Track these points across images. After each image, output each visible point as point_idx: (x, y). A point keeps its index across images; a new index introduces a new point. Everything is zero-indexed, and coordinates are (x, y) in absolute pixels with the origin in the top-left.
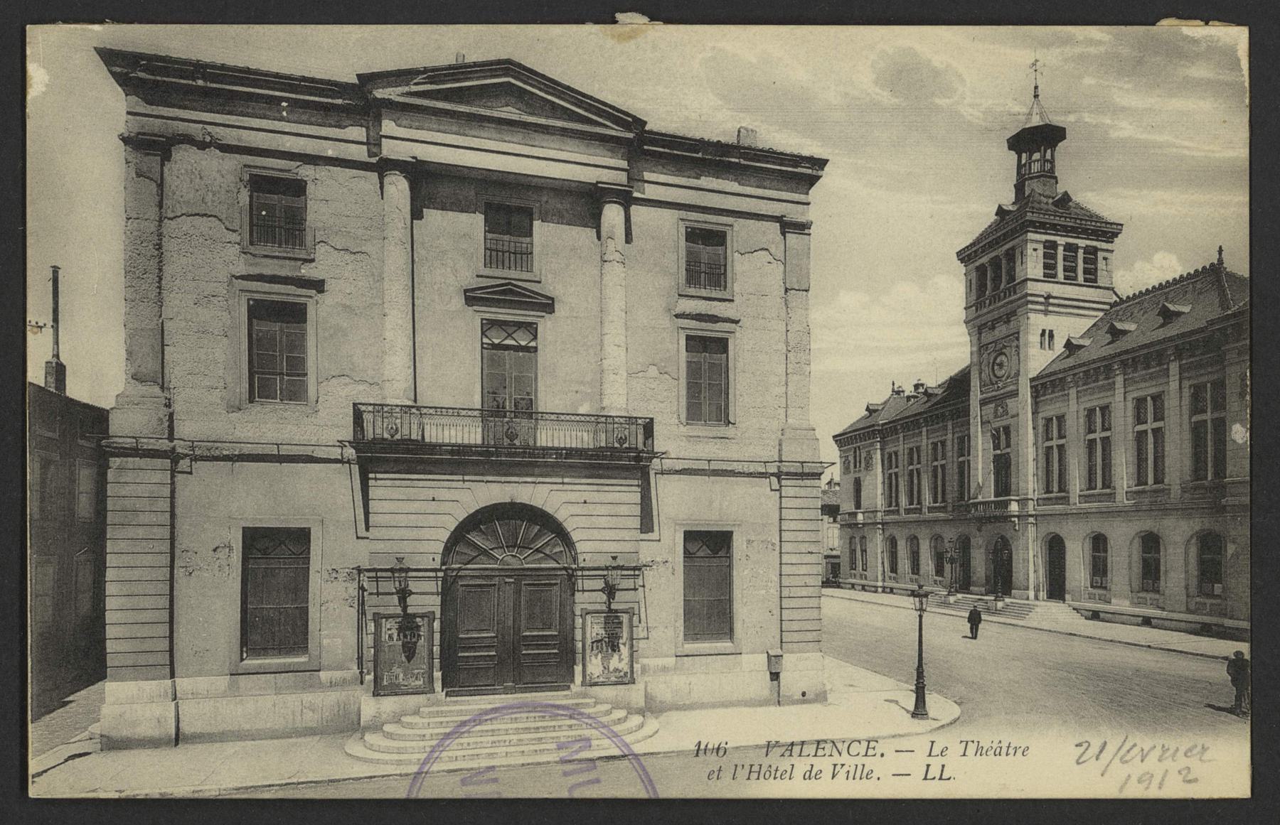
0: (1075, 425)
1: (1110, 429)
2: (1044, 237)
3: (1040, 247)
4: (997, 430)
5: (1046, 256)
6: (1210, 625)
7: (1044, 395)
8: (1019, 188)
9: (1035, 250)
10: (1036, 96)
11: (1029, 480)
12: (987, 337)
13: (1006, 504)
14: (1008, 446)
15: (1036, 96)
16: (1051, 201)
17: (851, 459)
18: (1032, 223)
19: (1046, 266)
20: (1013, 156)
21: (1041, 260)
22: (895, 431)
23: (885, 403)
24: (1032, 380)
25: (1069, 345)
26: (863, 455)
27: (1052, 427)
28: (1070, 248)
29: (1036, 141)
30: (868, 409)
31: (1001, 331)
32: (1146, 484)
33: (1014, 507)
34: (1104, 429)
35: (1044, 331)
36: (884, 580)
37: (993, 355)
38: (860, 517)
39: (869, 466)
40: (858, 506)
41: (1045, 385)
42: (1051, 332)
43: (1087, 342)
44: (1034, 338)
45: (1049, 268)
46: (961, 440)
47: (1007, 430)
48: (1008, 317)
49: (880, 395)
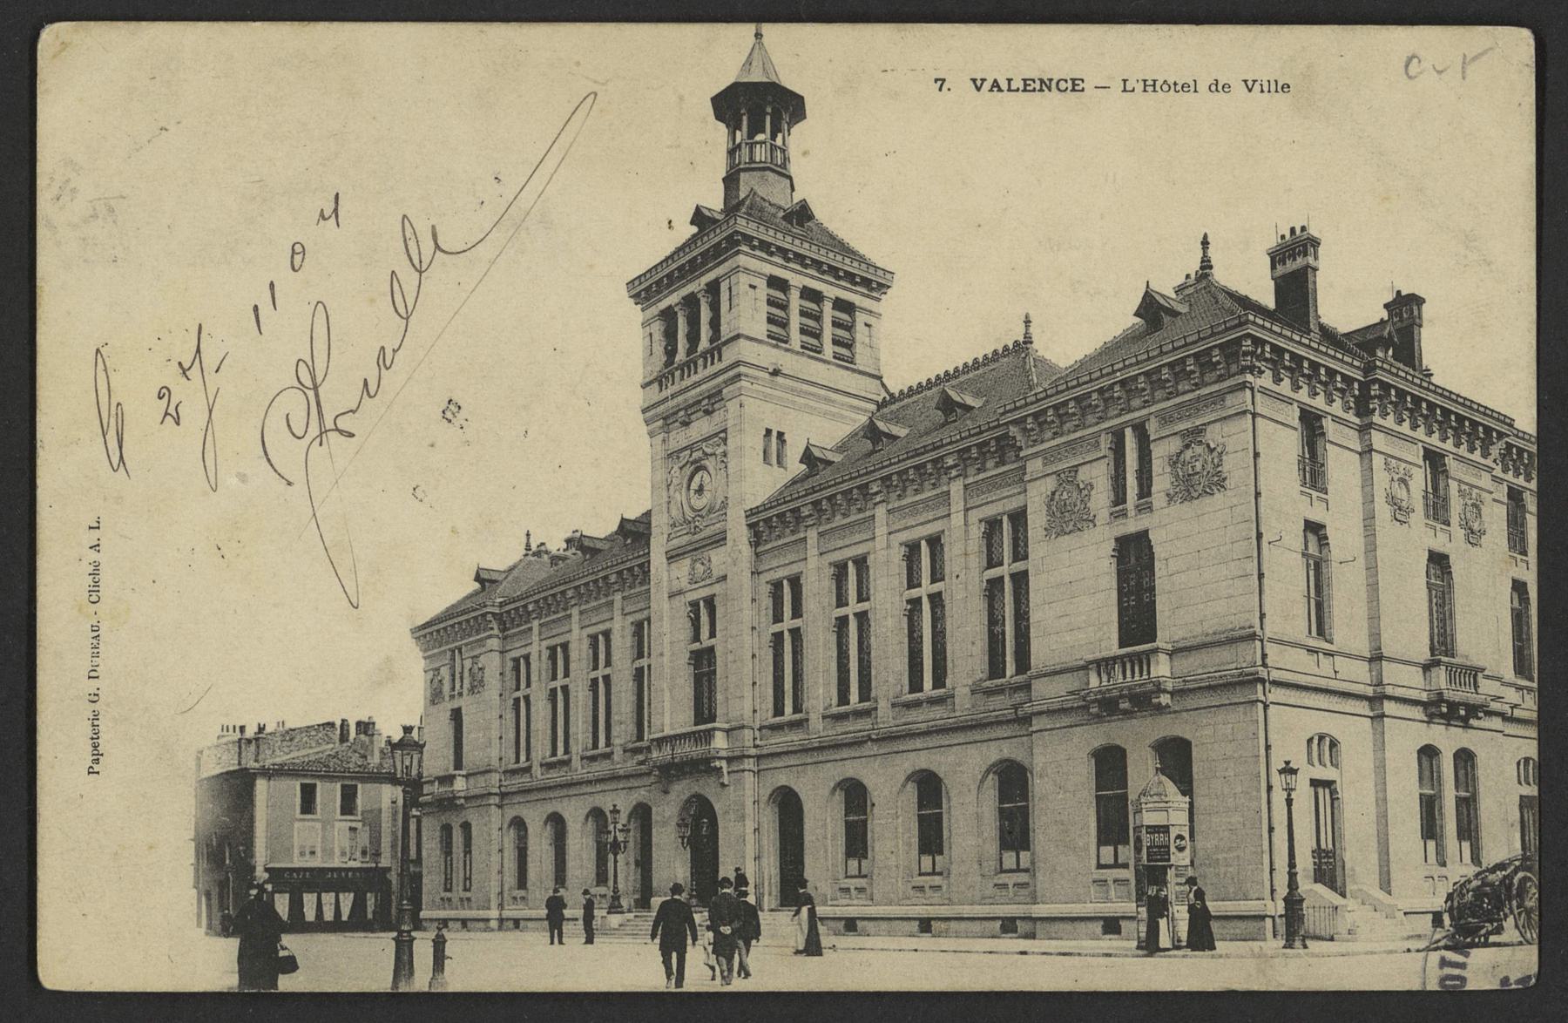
0: (818, 586)
1: (868, 599)
2: (769, 269)
3: (761, 283)
4: (694, 605)
6: (1013, 919)
8: (731, 181)
9: (753, 287)
11: (745, 694)
12: (679, 438)
13: (708, 736)
16: (781, 214)
18: (748, 239)
20: (722, 127)
21: (764, 308)
22: (526, 616)
23: (511, 569)
24: (751, 513)
25: (808, 457)
26: (468, 664)
27: (787, 595)
29: (757, 108)
30: (478, 578)
31: (702, 427)
32: (921, 690)
33: (720, 742)
34: (860, 599)
35: (769, 432)
36: (501, 906)
37: (688, 470)
38: (460, 784)
39: (477, 686)
40: (458, 764)
41: (769, 524)
42: (780, 435)
43: (837, 458)
44: (754, 441)
46: (639, 629)
47: (710, 602)
48: (712, 402)
49: (503, 555)
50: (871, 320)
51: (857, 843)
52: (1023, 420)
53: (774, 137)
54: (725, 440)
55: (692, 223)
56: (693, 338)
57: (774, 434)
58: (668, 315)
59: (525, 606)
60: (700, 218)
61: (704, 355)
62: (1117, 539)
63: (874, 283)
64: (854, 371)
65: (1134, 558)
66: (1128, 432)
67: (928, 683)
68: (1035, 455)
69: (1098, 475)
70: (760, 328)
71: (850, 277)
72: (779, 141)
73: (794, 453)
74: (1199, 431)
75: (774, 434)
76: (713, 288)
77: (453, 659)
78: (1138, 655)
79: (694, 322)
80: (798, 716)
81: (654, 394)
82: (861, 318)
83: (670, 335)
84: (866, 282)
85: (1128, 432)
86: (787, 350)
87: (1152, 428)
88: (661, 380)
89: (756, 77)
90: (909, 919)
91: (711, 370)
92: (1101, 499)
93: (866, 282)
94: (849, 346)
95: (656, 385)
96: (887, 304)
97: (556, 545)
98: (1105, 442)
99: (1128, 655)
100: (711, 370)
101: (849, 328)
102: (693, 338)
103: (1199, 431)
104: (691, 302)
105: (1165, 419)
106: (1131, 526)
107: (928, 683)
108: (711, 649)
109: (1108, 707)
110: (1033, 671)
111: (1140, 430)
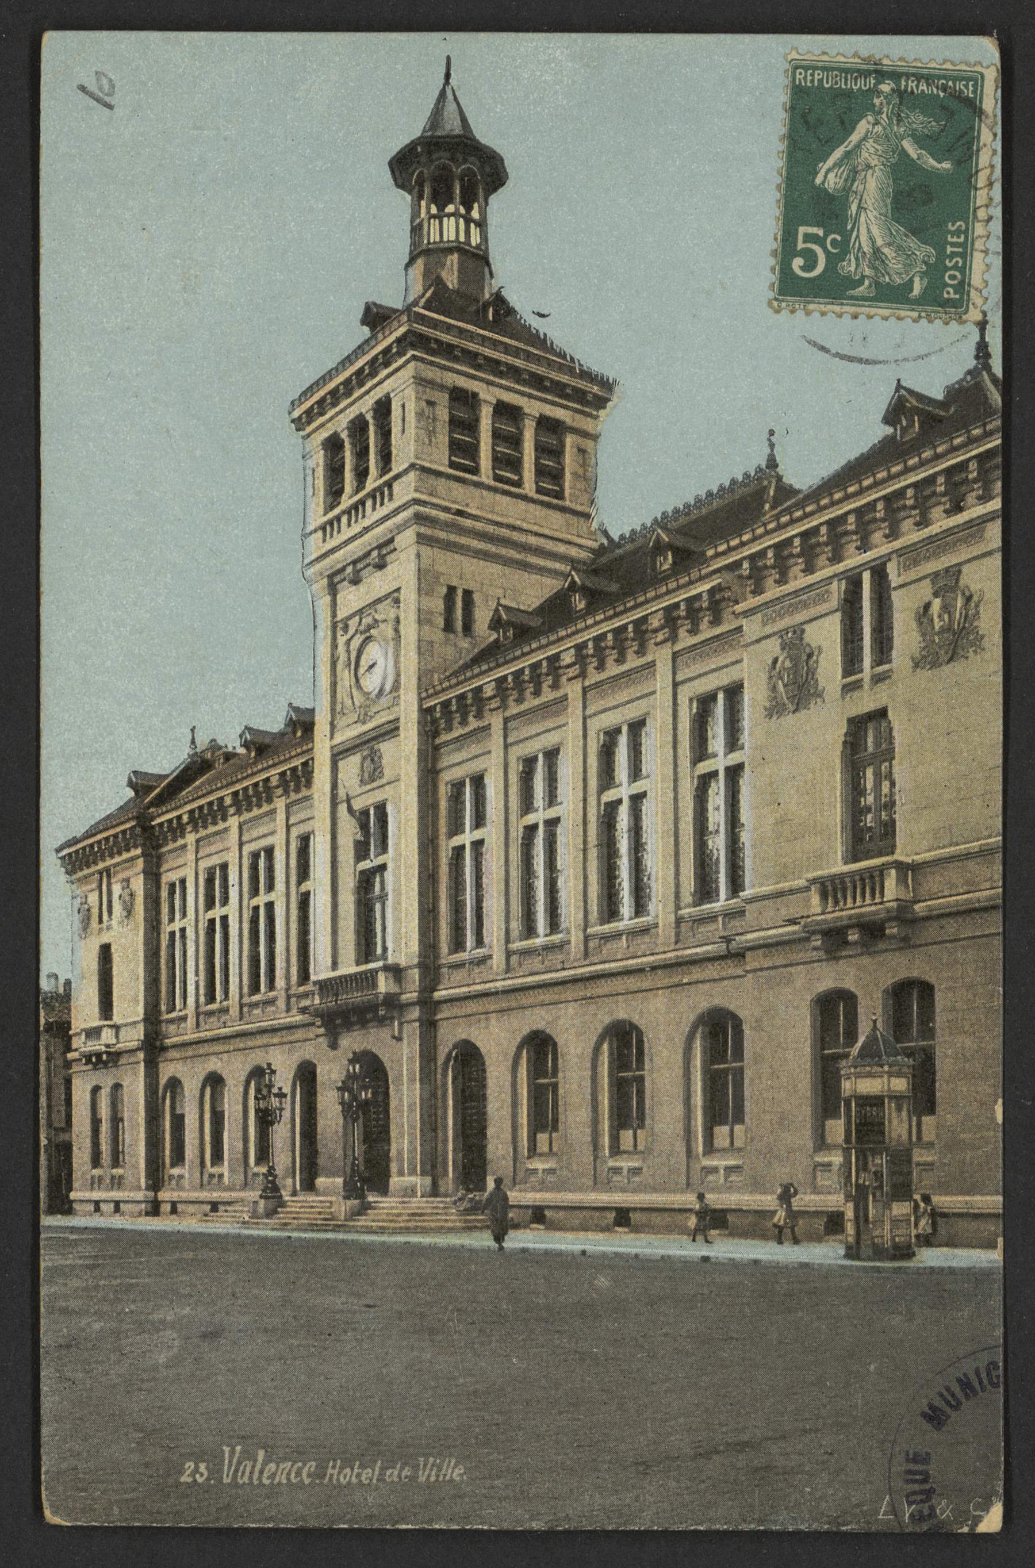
5: (454, 423)
7: (449, 728)
10: (448, 76)
12: (351, 599)
14: (384, 847)
15: (448, 76)
17: (93, 899)
19: (455, 446)
26: (117, 889)
28: (504, 411)
29: (449, 167)
30: (130, 784)
35: (452, 590)
42: (468, 594)
45: (463, 451)
50: (589, 444)
51: (544, 1113)
52: (737, 565)
53: (469, 209)
54: (397, 601)
55: (364, 322)
56: (362, 474)
57: (460, 593)
58: (333, 445)
59: (179, 817)
60: (376, 318)
61: (372, 495)
62: (851, 721)
63: (591, 393)
64: (563, 510)
65: (866, 741)
66: (866, 576)
67: (626, 908)
68: (748, 613)
69: (826, 635)
70: (440, 458)
71: (559, 389)
72: (475, 214)
73: (482, 616)
74: (954, 572)
75: (460, 593)
76: (383, 408)
77: (101, 880)
78: (870, 870)
79: (362, 453)
80: (480, 952)
81: (316, 545)
82: (569, 440)
83: (334, 471)
84: (580, 396)
85: (866, 576)
86: (478, 485)
87: (892, 568)
88: (328, 528)
89: (451, 125)
90: (202, 1202)
91: (382, 512)
92: (830, 668)
93: (580, 396)
94: (557, 476)
95: (320, 534)
96: (609, 422)
97: (232, 742)
98: (837, 590)
99: (860, 872)
100: (382, 512)
101: (557, 453)
102: (362, 474)
103: (954, 572)
104: (358, 427)
105: (911, 555)
106: (865, 702)
107: (626, 908)
108: (383, 867)
109: (834, 940)
110: (747, 893)
111: (879, 573)
